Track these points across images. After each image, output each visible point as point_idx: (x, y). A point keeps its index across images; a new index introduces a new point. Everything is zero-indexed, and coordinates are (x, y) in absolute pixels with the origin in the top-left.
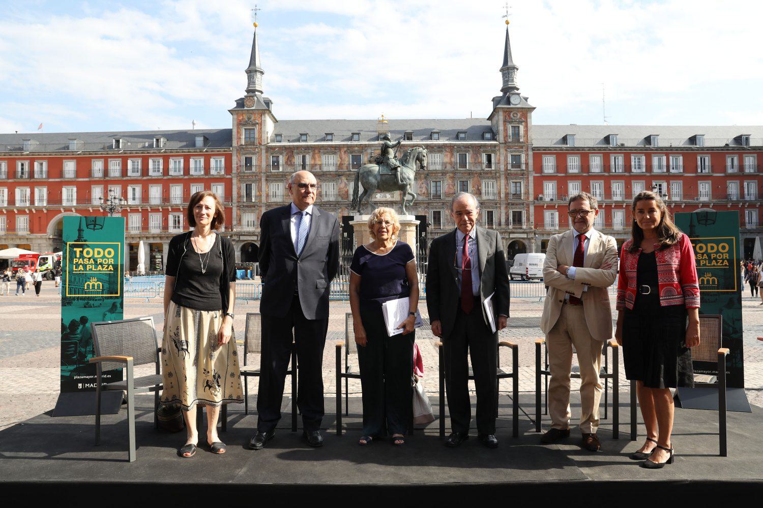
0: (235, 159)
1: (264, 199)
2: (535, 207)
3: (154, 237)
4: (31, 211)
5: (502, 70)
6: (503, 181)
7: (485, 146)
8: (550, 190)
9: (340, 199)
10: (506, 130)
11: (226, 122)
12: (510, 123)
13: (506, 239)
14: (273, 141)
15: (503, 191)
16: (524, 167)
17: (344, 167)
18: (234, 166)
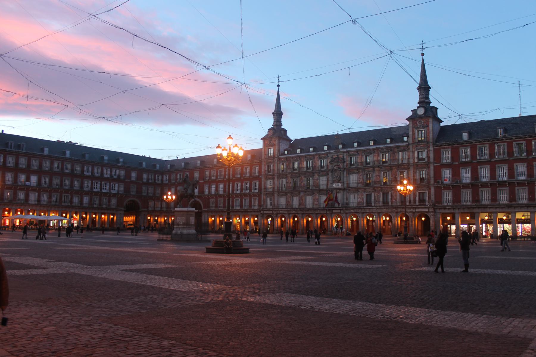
2: (435, 189)
5: (418, 89)
9: (314, 188)
11: (259, 145)
12: (417, 128)
16: (426, 160)
18: (263, 170)
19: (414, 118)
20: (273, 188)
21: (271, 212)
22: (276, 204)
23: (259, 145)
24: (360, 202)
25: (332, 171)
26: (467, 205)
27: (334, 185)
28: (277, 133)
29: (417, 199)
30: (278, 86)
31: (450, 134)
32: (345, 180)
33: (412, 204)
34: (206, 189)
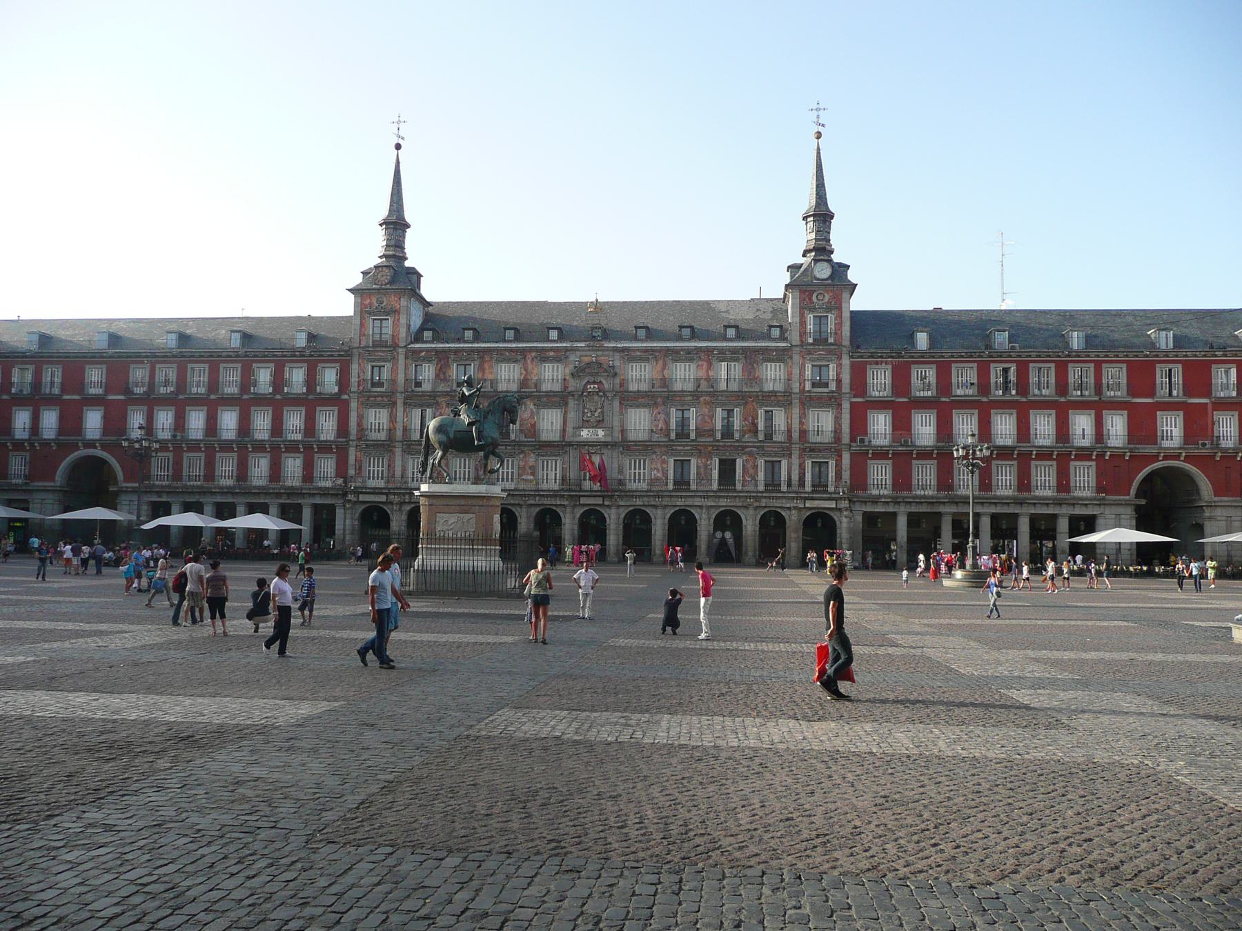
0: (354, 368)
1: (399, 434)
2: (853, 455)
3: (222, 493)
4: (32, 445)
6: (796, 411)
7: (766, 349)
8: (880, 425)
9: (523, 438)
10: (803, 323)
12: (811, 310)
13: (800, 509)
14: (418, 338)
15: (796, 426)
16: (833, 386)
17: (531, 383)
18: (354, 380)
19: (800, 283)
20: (391, 431)
21: (383, 498)
22: (398, 474)
23: (345, 306)
24: (657, 479)
25: (582, 395)
26: (924, 497)
27: (585, 434)
28: (393, 280)
29: (808, 477)
30: (398, 147)
31: (885, 332)
32: (616, 424)
33: (795, 488)
34: (136, 419)
